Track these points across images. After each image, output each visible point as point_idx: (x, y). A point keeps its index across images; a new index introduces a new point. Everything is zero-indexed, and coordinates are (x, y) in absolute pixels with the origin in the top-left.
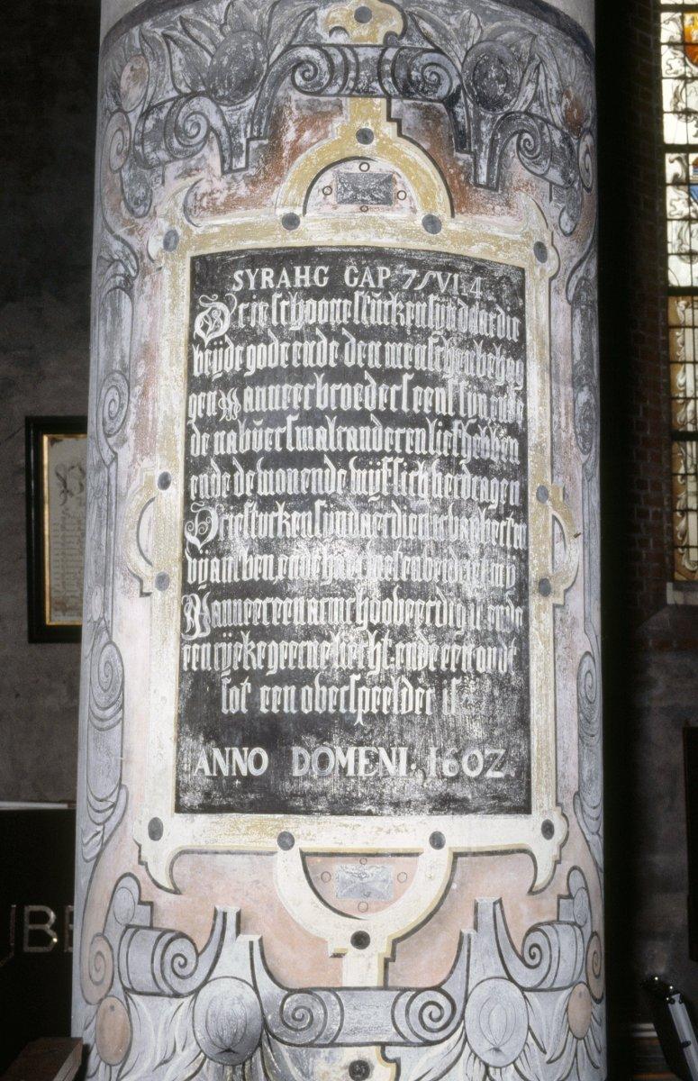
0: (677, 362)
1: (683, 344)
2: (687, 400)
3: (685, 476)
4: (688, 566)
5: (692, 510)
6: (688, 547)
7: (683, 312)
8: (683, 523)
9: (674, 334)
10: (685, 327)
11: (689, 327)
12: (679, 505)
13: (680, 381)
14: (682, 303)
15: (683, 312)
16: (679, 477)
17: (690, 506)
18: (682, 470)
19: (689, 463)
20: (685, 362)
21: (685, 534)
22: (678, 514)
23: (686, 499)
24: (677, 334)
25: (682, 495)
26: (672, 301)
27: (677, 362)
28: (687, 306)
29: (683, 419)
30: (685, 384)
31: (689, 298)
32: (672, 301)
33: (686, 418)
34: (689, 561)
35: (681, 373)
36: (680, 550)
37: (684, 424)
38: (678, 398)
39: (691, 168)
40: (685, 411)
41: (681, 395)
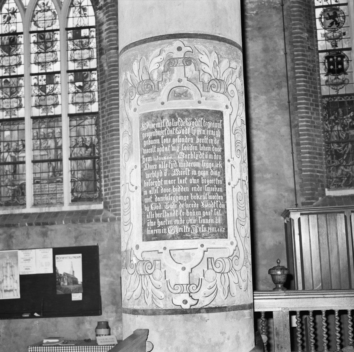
39: (3, 83)
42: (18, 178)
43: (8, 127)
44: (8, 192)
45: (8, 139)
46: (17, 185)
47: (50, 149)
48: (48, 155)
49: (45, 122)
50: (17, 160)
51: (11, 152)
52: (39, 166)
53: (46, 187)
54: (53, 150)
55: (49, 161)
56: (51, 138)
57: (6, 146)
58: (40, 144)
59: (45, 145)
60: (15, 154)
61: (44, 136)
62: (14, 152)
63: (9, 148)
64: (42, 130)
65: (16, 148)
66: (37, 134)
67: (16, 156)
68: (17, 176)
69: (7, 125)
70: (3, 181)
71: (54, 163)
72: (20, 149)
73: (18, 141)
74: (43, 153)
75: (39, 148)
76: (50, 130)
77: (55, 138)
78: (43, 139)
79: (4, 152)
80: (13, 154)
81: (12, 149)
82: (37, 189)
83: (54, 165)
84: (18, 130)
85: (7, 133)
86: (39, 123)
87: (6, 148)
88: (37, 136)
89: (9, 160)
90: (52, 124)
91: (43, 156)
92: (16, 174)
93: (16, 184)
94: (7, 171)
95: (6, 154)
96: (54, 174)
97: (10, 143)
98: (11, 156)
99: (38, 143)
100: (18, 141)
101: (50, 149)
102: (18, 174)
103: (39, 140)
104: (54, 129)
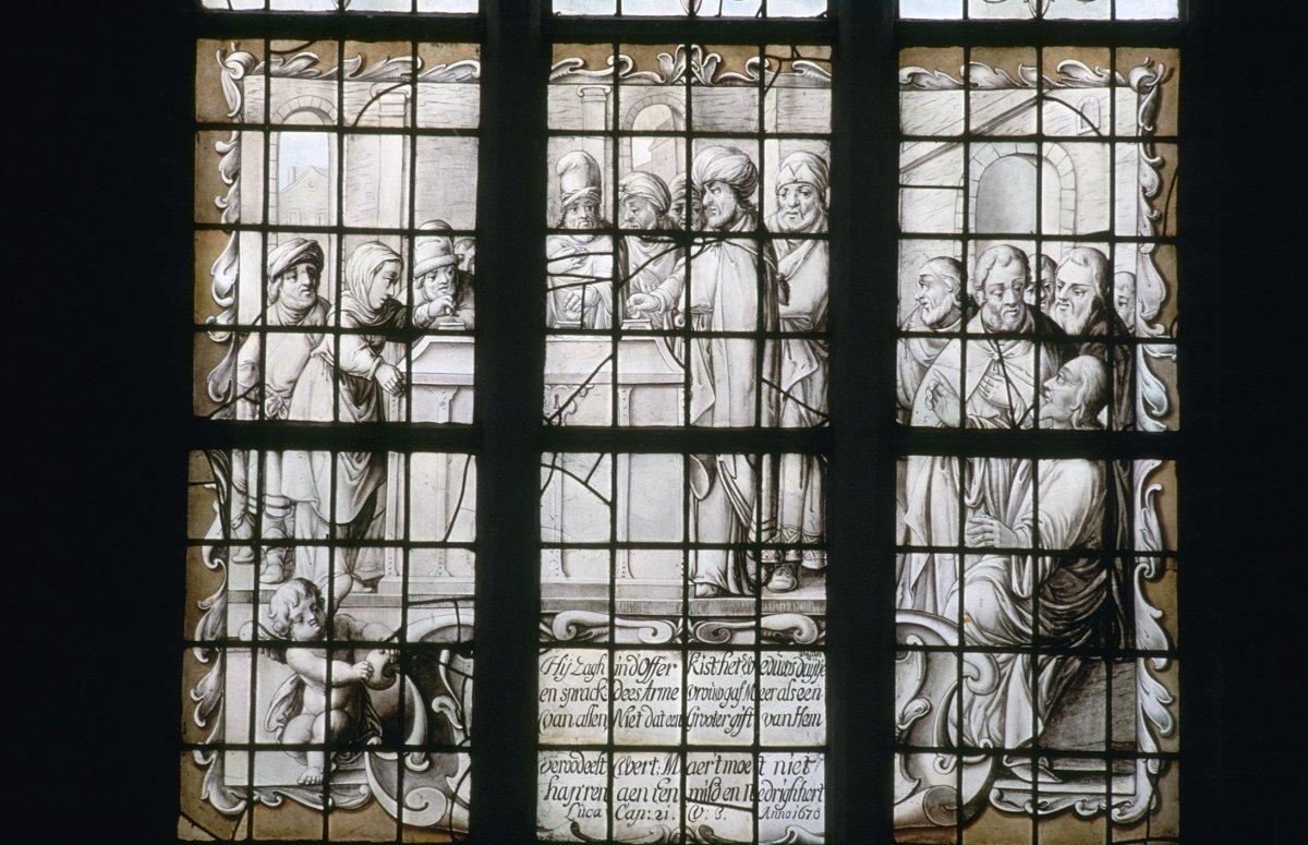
0: (217, 227)
1: (236, 175)
2: (239, 332)
3: (221, 547)
4: (217, 802)
5: (237, 643)
6: (221, 747)
7: (239, 83)
8: (210, 680)
9: (210, 148)
10: (242, 127)
11: (253, 127)
12: (203, 628)
13: (223, 280)
14: (236, 59)
15: (239, 83)
16: (206, 550)
17: (231, 633)
18: (215, 532)
19: (236, 511)
20: (238, 227)
21: (214, 711)
22: (198, 653)
23: (224, 613)
24: (220, 146)
25: (214, 602)
26: (207, 49)
27: (217, 227)
28: (248, 69)
29: (223, 388)
30: (235, 289)
31: (259, 44)
32: (207, 49)
33: (233, 383)
34: (223, 794)
35: (224, 258)
36: (198, 756)
37: (227, 404)
38: (214, 327)
40: (233, 363)
41: (222, 320)
42: (391, 586)
43: (316, 93)
44: (295, 703)
45: (306, 203)
46: (382, 645)
47: (710, 335)
48: (687, 384)
49: (668, 81)
50: (394, 414)
51: (338, 331)
52: (602, 482)
53: (658, 682)
54: (744, 349)
55: (696, 443)
56: (723, 234)
57: (291, 268)
58: (620, 282)
59: (668, 289)
60: (377, 350)
61: (661, 213)
62: (360, 329)
63: (313, 287)
64: (639, 150)
65: (390, 302)
66: (595, 182)
67: (387, 377)
68: (392, 556)
69: (300, 75)
70: (254, 598)
71: (738, 468)
72: (421, 314)
73: (410, 233)
74: (640, 361)
75: (603, 319)
76: (715, 161)
77: (762, 237)
78: (647, 236)
79: (264, 329)
80: (355, 355)
81: (346, 303)
82: (575, 694)
83: (744, 482)
84: (412, 131)
85: (304, 154)
86: (617, 82)
87: (293, 292)
88: (594, 203)
89: (315, 403)
90: (734, 105)
91: (642, 396)
92: (381, 543)
93: (376, 633)
94: (290, 505)
95: (286, 352)
96: (740, 566)
97: (327, 244)
98: (338, 374)
99: (604, 266)
100: (410, 233)
101: (710, 335)
102: (394, 544)
103: (605, 243)
104: (750, 147)
